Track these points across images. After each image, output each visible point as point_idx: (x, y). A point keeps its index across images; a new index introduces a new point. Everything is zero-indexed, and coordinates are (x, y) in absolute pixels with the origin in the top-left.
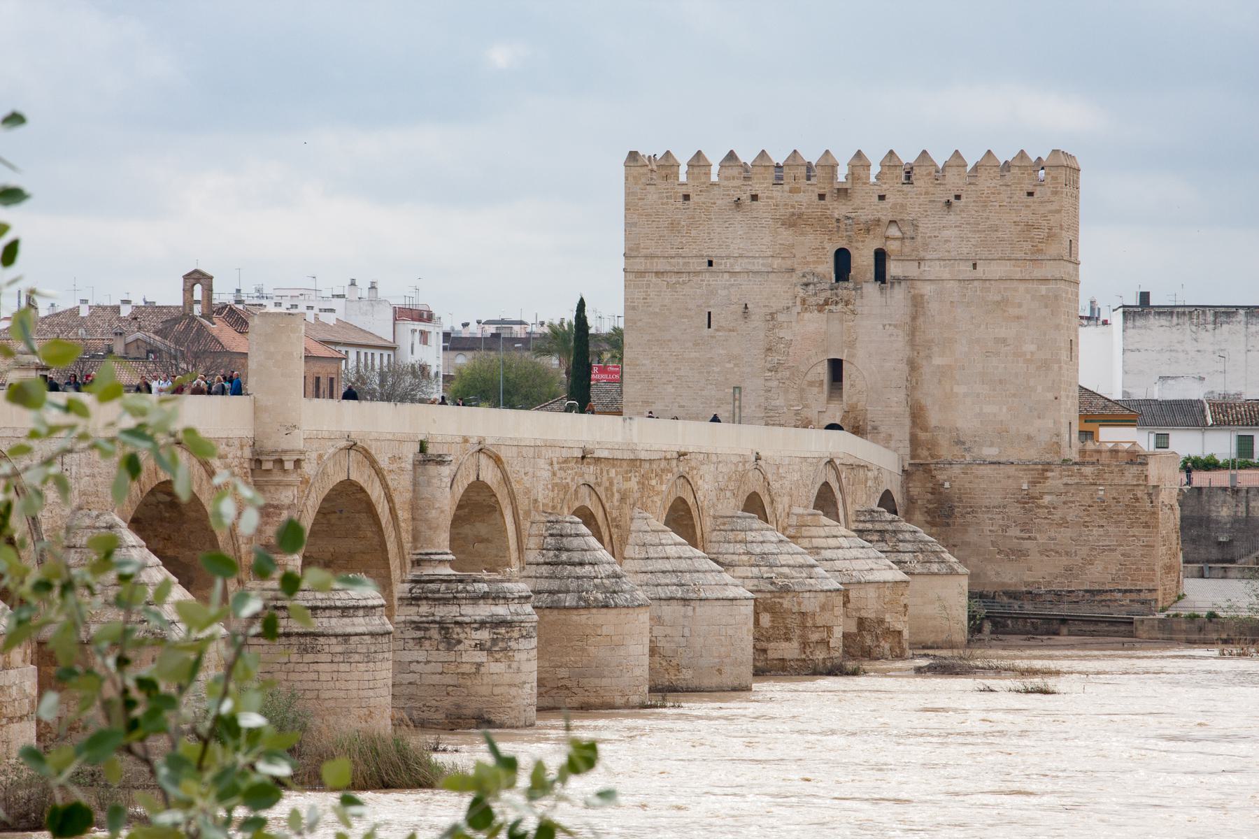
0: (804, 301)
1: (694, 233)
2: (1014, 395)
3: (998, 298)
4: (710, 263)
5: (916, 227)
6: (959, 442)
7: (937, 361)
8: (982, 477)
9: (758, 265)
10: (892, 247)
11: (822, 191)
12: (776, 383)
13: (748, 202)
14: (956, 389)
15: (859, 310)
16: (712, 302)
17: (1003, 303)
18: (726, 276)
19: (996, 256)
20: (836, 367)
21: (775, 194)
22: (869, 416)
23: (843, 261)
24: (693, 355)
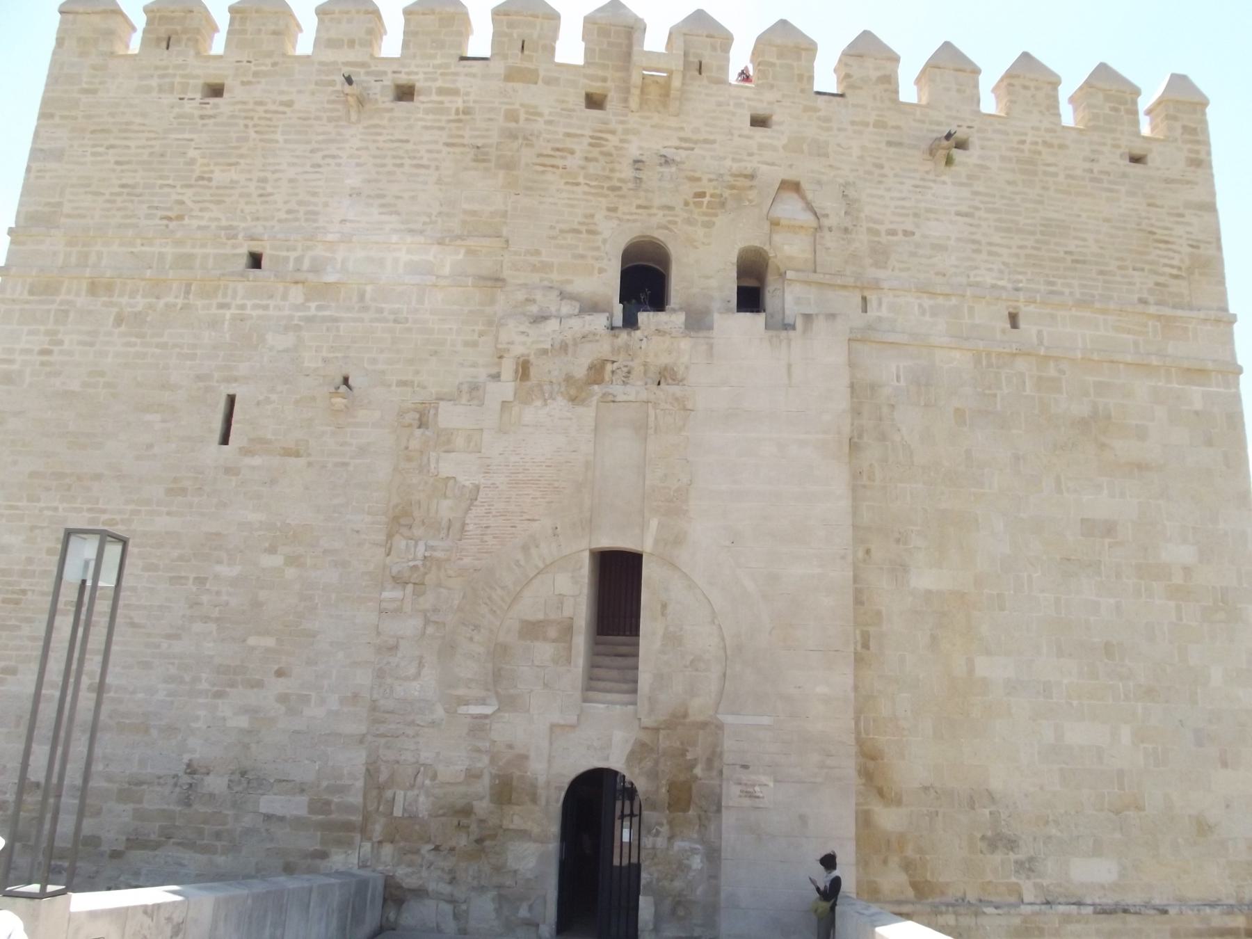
0: (524, 370)
4: (256, 261)
5: (851, 206)
6: (999, 841)
7: (924, 579)
10: (788, 250)
11: (596, 87)
13: (385, 100)
14: (983, 668)
20: (618, 577)
21: (461, 84)
22: (728, 744)
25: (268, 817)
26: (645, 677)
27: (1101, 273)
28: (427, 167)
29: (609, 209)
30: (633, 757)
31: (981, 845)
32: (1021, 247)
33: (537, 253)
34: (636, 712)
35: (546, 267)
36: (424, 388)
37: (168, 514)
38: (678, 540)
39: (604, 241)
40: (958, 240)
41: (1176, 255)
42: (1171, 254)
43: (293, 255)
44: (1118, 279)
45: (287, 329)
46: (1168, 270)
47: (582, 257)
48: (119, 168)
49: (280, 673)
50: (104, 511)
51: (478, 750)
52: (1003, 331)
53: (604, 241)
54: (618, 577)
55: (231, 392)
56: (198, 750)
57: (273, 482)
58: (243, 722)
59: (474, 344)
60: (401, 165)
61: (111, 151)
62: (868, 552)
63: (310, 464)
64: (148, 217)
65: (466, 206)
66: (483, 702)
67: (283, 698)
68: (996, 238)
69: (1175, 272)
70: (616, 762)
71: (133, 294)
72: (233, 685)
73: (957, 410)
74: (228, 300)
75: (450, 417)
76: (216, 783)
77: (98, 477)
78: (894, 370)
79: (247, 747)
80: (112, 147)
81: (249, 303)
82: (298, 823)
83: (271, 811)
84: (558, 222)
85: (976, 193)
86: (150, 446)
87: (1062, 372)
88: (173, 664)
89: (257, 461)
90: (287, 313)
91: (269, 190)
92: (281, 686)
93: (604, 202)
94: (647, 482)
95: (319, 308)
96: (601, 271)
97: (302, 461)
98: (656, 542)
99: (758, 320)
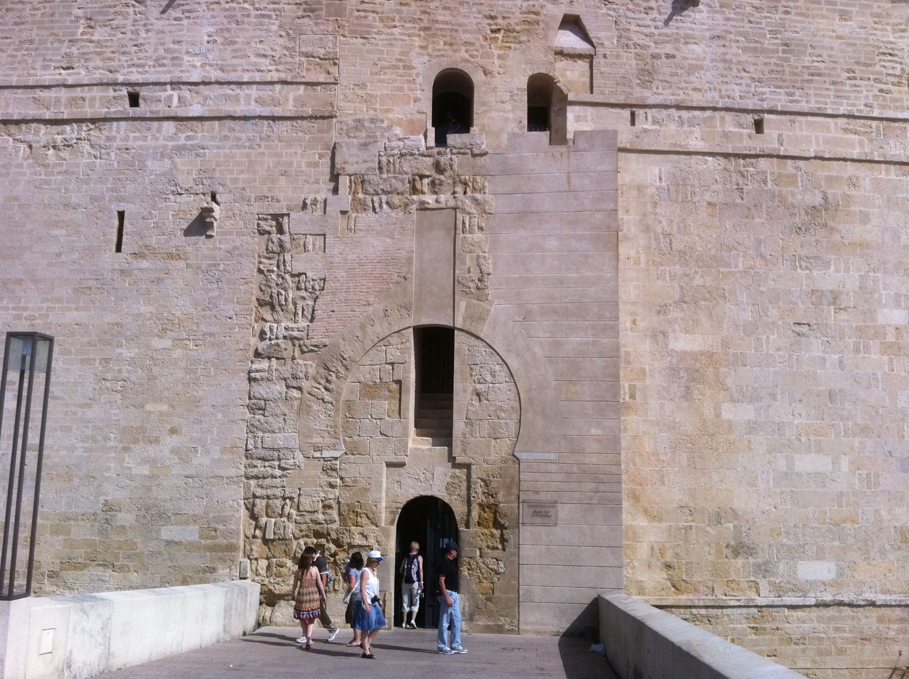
1: (99, 34)
2: (865, 430)
3: (818, 200)
4: (134, 100)
8: (802, 640)
9: (247, 102)
10: (569, 77)
12: (280, 387)
14: (728, 412)
15: (493, 203)
16: (131, 187)
17: (822, 215)
18: (169, 127)
19: (804, 107)
23: (453, 103)
24: (72, 316)
25: (169, 543)
26: (459, 426)
27: (834, 83)
28: (270, 17)
29: (421, 47)
30: (449, 487)
31: (728, 552)
32: (766, 64)
33: (363, 86)
34: (450, 452)
35: (368, 100)
36: (278, 201)
37: (77, 309)
38: (482, 319)
39: (417, 75)
40: (713, 61)
41: (898, 66)
42: (896, 65)
43: (163, 95)
44: (847, 88)
45: (162, 156)
46: (890, 79)
47: (401, 89)
48: (17, 28)
49: (173, 431)
50: (25, 309)
51: (332, 486)
52: (750, 136)
53: (417, 75)
54: (435, 350)
55: (121, 209)
56: (112, 494)
57: (159, 280)
58: (145, 470)
59: (316, 165)
60: (248, 16)
61: (10, 14)
62: (634, 322)
63: (188, 266)
64: (45, 68)
65: (303, 49)
66: (334, 447)
67: (175, 451)
68: (744, 57)
69: (896, 80)
70: (438, 490)
71: (37, 132)
72: (136, 441)
73: (709, 204)
74: (114, 134)
75: (296, 222)
76: (125, 518)
77: (19, 282)
78: (657, 171)
79: (149, 489)
80: (7, 10)
81: (132, 135)
82: (191, 547)
83: (170, 538)
84: (379, 59)
85: (728, 19)
86: (59, 255)
87: (798, 168)
88: (88, 427)
89: (144, 264)
90: (161, 142)
91: (141, 41)
92: (173, 441)
93: (417, 42)
94: (457, 272)
95: (188, 138)
96: (416, 100)
97: (182, 264)
98: (464, 321)
99: (544, 136)
